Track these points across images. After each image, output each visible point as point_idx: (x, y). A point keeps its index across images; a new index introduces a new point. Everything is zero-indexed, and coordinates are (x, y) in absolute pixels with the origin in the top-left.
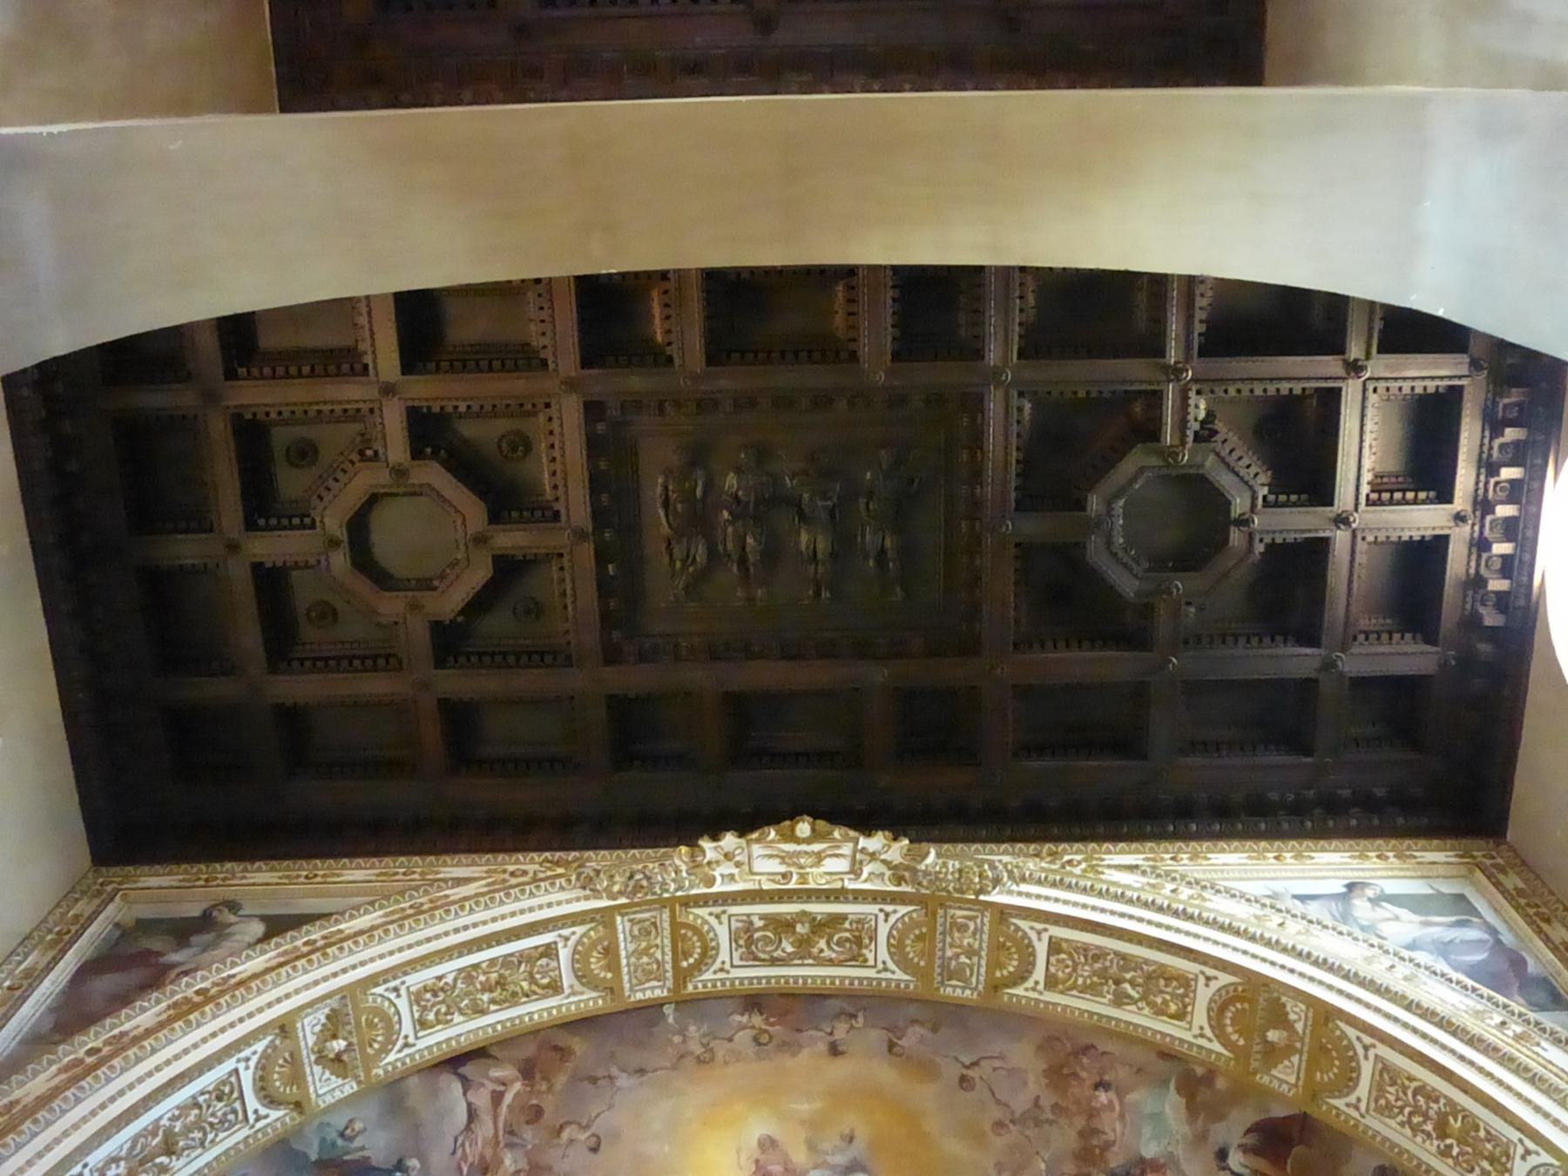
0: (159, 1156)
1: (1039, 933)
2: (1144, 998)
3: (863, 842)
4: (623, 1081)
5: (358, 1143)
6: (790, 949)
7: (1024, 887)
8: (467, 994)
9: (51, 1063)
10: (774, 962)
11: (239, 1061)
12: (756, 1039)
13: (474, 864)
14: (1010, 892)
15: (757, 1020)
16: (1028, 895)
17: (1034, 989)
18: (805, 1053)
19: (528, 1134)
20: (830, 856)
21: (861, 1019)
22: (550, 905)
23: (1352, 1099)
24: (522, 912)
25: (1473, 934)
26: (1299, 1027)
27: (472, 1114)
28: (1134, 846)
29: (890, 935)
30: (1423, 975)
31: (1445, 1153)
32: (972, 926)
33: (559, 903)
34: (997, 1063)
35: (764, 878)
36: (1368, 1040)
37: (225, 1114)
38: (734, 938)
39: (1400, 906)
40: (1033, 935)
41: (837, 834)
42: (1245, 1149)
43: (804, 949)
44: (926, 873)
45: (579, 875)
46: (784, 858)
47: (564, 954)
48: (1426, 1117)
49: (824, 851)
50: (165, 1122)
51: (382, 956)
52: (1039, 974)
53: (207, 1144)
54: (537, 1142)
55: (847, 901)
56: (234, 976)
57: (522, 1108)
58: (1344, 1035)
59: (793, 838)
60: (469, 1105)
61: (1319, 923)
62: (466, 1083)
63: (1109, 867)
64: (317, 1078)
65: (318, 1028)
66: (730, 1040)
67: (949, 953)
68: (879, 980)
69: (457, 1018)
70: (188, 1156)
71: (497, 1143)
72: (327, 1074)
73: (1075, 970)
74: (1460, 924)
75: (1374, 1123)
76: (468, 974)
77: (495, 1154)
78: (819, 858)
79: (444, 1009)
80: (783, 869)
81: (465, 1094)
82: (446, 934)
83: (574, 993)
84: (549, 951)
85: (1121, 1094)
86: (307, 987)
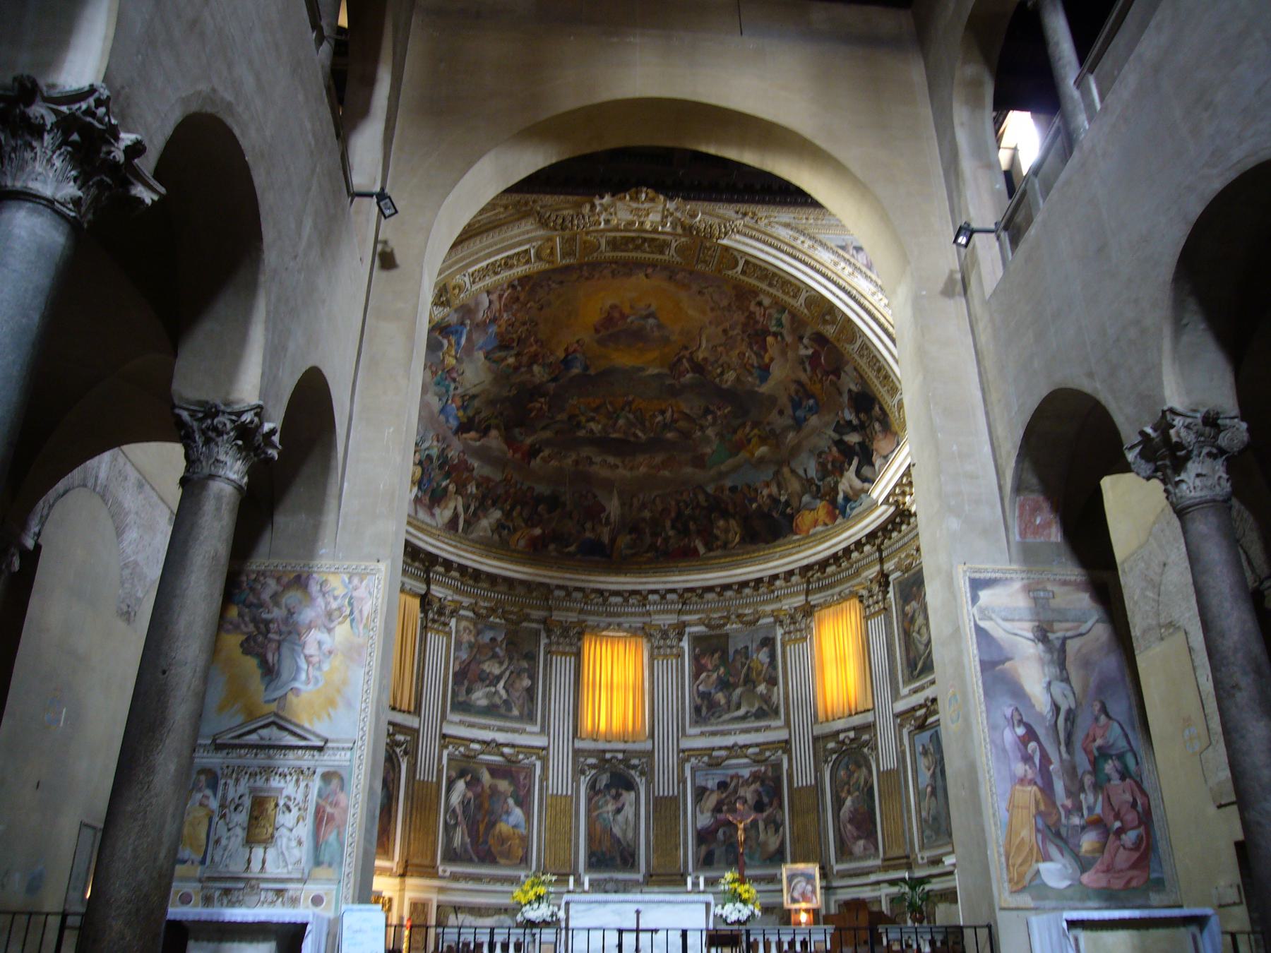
4: (554, 285)
7: (738, 237)
10: (626, 251)
12: (613, 272)
27: (490, 302)
28: (792, 209)
38: (608, 243)
42: (810, 339)
43: (637, 248)
52: (739, 268)
59: (635, 198)
63: (777, 223)
77: (500, 314)
84: (527, 252)
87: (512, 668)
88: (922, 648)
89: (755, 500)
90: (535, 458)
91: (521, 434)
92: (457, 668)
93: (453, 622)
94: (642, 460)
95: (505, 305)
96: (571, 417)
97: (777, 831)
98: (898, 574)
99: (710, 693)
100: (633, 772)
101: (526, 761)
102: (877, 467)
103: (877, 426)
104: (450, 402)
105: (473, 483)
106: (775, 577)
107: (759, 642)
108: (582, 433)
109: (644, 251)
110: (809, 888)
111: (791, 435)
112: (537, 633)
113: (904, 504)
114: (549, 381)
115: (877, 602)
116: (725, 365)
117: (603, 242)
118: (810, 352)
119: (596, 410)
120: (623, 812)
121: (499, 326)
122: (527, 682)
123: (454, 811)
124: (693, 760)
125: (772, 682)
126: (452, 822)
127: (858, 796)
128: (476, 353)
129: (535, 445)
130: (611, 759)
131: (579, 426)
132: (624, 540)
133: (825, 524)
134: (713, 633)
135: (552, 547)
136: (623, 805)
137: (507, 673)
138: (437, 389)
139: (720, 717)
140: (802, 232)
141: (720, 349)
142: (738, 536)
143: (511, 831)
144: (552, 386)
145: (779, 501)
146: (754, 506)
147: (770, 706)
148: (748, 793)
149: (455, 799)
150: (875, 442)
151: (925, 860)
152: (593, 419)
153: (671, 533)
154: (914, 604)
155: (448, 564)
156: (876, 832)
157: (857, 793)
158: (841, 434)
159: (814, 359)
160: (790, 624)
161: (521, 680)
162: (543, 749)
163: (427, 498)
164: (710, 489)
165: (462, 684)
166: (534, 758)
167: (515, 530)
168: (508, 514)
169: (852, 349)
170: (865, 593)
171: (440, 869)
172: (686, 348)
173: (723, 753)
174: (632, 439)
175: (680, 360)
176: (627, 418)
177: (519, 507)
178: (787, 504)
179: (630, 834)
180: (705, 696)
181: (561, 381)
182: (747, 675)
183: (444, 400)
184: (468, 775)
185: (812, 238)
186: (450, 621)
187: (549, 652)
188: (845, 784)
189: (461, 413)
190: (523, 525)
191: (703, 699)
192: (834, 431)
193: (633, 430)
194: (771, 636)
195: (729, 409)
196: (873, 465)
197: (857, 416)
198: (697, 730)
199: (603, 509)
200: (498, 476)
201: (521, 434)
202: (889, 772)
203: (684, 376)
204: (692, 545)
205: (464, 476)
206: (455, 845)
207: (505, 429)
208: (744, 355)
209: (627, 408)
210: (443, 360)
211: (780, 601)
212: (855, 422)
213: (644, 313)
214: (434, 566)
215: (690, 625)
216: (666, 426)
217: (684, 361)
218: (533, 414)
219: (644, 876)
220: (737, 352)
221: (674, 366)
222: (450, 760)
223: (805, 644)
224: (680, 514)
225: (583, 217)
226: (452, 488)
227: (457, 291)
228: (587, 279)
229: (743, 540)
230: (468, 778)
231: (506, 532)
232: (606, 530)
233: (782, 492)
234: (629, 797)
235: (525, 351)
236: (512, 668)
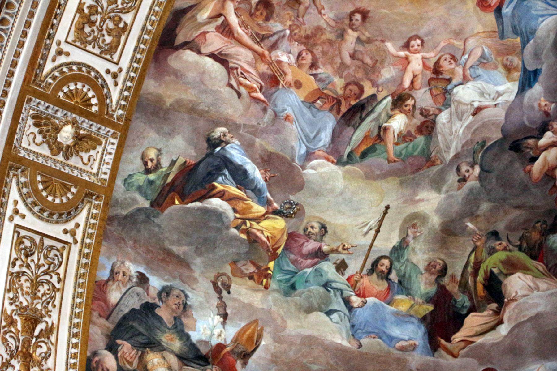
0: (34, 330)
5: (165, 163)
11: (11, 219)
19: (276, 26)
37: (46, 257)
53: (58, 286)
54: (289, 23)
57: (251, 15)
60: (212, 56)
64: (80, 166)
65: (39, 138)
69: (127, 18)
70: (54, 306)
71: (262, 56)
72: (85, 156)
77: (270, 64)
79: (111, 25)
81: (199, 52)
95: (261, 39)
104: (356, 301)
114: (522, 89)
121: (298, 85)
138: (296, 299)
144: (537, 89)
181: (544, 68)
183: (338, 304)
207: (534, 257)
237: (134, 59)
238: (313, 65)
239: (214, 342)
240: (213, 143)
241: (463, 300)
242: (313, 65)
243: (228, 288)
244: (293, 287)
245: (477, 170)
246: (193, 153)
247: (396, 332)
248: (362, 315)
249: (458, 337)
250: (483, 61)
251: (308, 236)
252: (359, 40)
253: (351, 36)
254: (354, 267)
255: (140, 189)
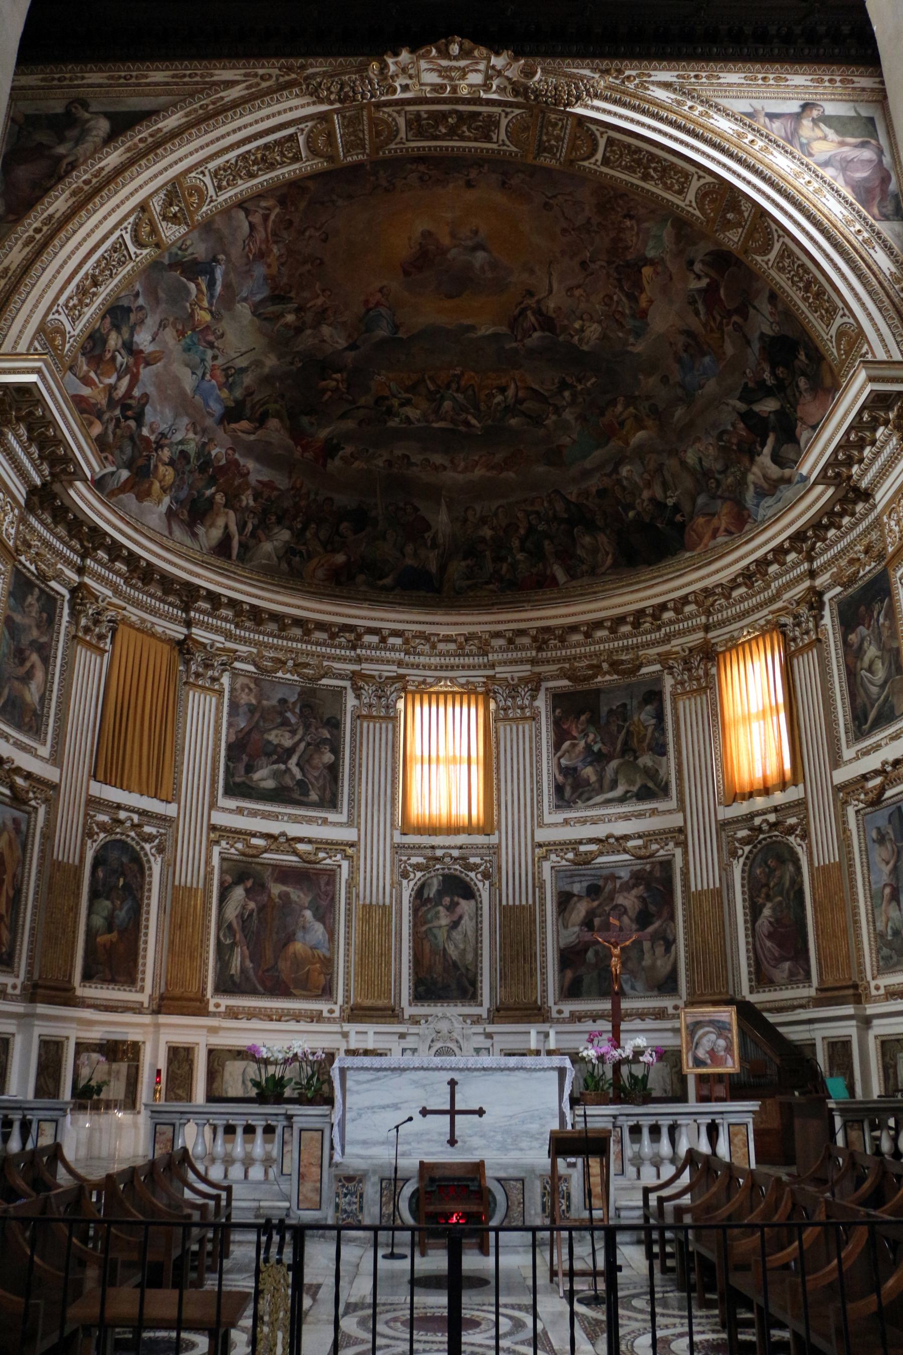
1: (602, 133)
2: (660, 179)
3: (494, 61)
4: (340, 202)
5: (190, 251)
6: (444, 131)
7: (597, 103)
8: (245, 167)
9: (17, 239)
10: (435, 138)
12: (421, 179)
13: (234, 67)
14: (586, 106)
15: (422, 168)
16: (598, 109)
17: (595, 164)
18: (451, 185)
19: (285, 235)
20: (472, 71)
21: (486, 167)
22: (291, 109)
23: (766, 258)
24: (274, 115)
25: (867, 154)
26: (746, 214)
27: (252, 226)
29: (508, 125)
30: (826, 190)
31: (805, 299)
32: (560, 123)
33: (297, 108)
34: (567, 198)
35: (428, 89)
36: (781, 233)
38: (408, 123)
39: (830, 127)
40: (598, 134)
41: (476, 53)
42: (702, 261)
43: (453, 133)
44: (534, 92)
45: (307, 88)
46: (441, 72)
47: (301, 139)
48: (801, 279)
49: (467, 66)
50: (91, 271)
51: (191, 154)
52: (599, 156)
55: (481, 105)
56: (102, 169)
58: (769, 226)
59: (444, 54)
60: (250, 223)
61: (775, 142)
62: (247, 212)
63: (653, 83)
66: (405, 178)
67: (545, 138)
68: (499, 151)
69: (240, 182)
73: (621, 156)
74: (863, 145)
75: (773, 273)
76: (244, 157)
78: (464, 72)
80: (439, 81)
82: (228, 134)
83: (308, 160)
84: (292, 138)
85: (639, 222)
86: (151, 179)
87: (308, 738)
88: (874, 690)
89: (631, 507)
90: (333, 459)
91: (312, 424)
92: (233, 738)
93: (226, 680)
94: (476, 458)
95: (275, 234)
96: (380, 400)
97: (668, 950)
98: (839, 589)
99: (575, 769)
100: (472, 875)
101: (328, 861)
102: (802, 444)
103: (802, 382)
104: (208, 377)
105: (249, 492)
106: (663, 607)
107: (640, 698)
108: (394, 423)
109: (462, 138)
110: (722, 1043)
111: (679, 412)
112: (339, 693)
113: (850, 477)
114: (346, 349)
115: (807, 632)
116: (585, 316)
117: (401, 122)
118: (704, 282)
119: (413, 388)
120: (460, 928)
121: (269, 266)
122: (328, 758)
123: (230, 926)
124: (553, 857)
125: (661, 750)
126: (228, 942)
127: (780, 903)
128: (238, 306)
129: (332, 439)
130: (443, 857)
131: (390, 412)
132: (457, 567)
133: (729, 532)
134: (579, 688)
135: (361, 578)
136: (461, 918)
137: (302, 745)
139: (589, 799)
140: (689, 94)
141: (577, 292)
142: (610, 556)
143: (310, 952)
144: (352, 354)
145: (666, 505)
146: (631, 514)
147: (657, 785)
148: (629, 901)
149: (231, 913)
150: (799, 408)
151: (882, 991)
152: (406, 403)
153: (520, 556)
154: (862, 630)
155: (213, 598)
156: (807, 950)
157: (780, 898)
158: (750, 402)
159: (710, 294)
160: (684, 670)
161: (323, 753)
162: (352, 845)
163: (186, 512)
164: (572, 493)
165: (240, 760)
166: (339, 857)
167: (310, 557)
168: (298, 535)
169: (766, 262)
170: (789, 620)
171: (212, 1002)
172: (530, 294)
173: (593, 847)
174: (462, 428)
175: (523, 312)
176: (454, 399)
177: (313, 526)
178: (677, 508)
179: (470, 957)
180: (566, 771)
182: (625, 743)
184: (248, 879)
185: (705, 102)
186: (221, 676)
187: (358, 717)
188: (763, 886)
189: (225, 394)
190: (320, 549)
191: (565, 776)
192: (740, 399)
193: (464, 415)
194: (657, 689)
195: (593, 380)
196: (797, 442)
197: (773, 373)
198: (559, 817)
199: (428, 527)
200: (282, 482)
201: (312, 424)
202: (825, 870)
203: (530, 336)
204: (548, 572)
205: (236, 483)
206: (233, 972)
208: (611, 298)
209: (454, 386)
210: (192, 315)
211: (669, 641)
212: (770, 381)
213: (470, 243)
214: (196, 602)
215: (547, 679)
216: (509, 410)
217: (529, 313)
218: (326, 397)
219: (489, 1011)
220: (601, 295)
221: (514, 323)
222: (223, 859)
223: (704, 698)
224: (531, 529)
225: (371, 83)
226: (220, 498)
227: (195, 199)
228: (387, 190)
229: (615, 565)
230: (249, 884)
231: (298, 558)
232: (433, 555)
233: (669, 493)
234: (466, 906)
235: (309, 305)
236: (308, 738)
237: (225, 200)
238: (282, 264)
239: (141, 347)
240: (215, 260)
241: (248, 412)
242: (282, 264)
243: (165, 327)
244: (189, 350)
245: (300, 365)
246: (204, 256)
247: (212, 403)
248: (205, 385)
249: (233, 426)
250: (344, 324)
251: (214, 333)
252: (309, 271)
253: (308, 267)
254: (220, 361)
255: (170, 254)
